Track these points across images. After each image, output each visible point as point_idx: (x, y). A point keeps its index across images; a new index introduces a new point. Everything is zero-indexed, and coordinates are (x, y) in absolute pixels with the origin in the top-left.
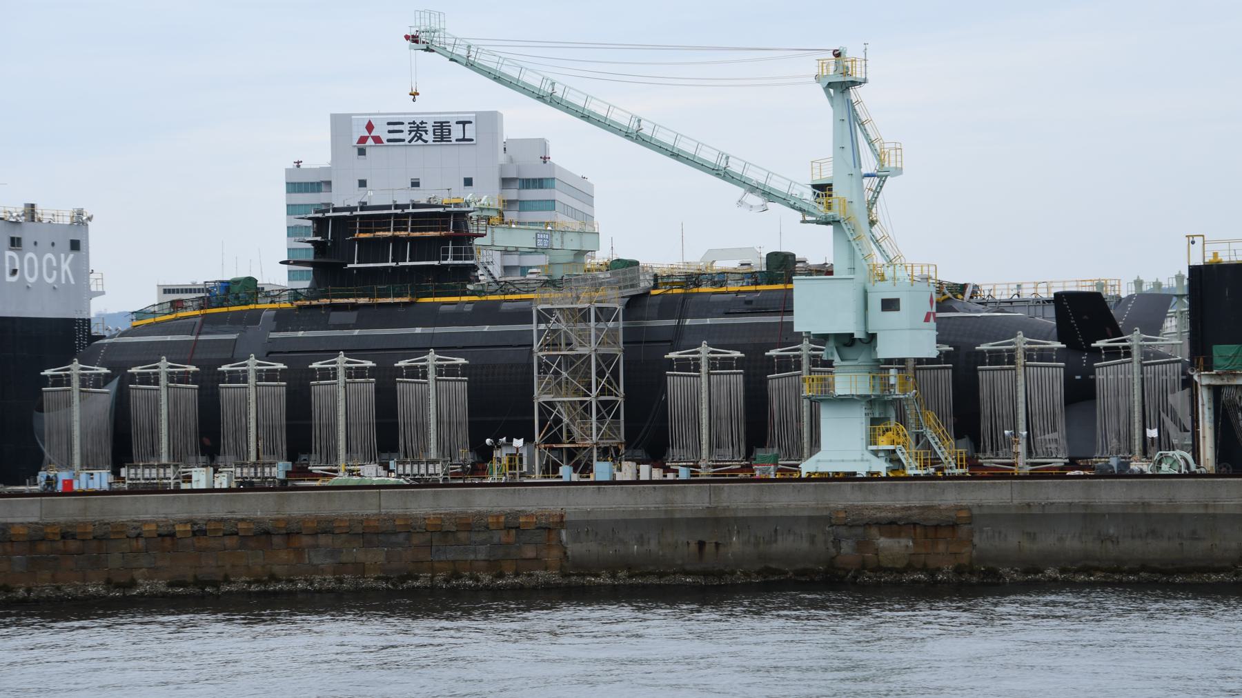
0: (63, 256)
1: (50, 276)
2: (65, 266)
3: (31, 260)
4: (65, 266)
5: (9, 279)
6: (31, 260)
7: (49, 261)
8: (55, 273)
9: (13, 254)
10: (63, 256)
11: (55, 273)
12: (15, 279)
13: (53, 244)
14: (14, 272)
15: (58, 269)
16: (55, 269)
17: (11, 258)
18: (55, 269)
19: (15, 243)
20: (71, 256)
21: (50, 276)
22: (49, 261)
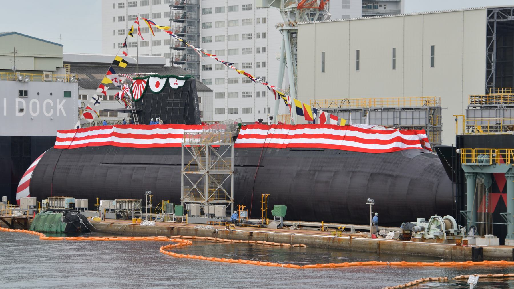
0: (58, 101)
1: (48, 112)
2: (60, 106)
3: (34, 104)
4: (60, 106)
5: (18, 114)
6: (34, 104)
7: (48, 104)
8: (52, 110)
9: (22, 100)
10: (58, 101)
11: (52, 110)
12: (22, 114)
13: (51, 94)
14: (22, 110)
15: (55, 108)
16: (52, 108)
17: (20, 102)
18: (52, 108)
19: (23, 94)
20: (65, 100)
21: (48, 112)
22: (48, 104)
